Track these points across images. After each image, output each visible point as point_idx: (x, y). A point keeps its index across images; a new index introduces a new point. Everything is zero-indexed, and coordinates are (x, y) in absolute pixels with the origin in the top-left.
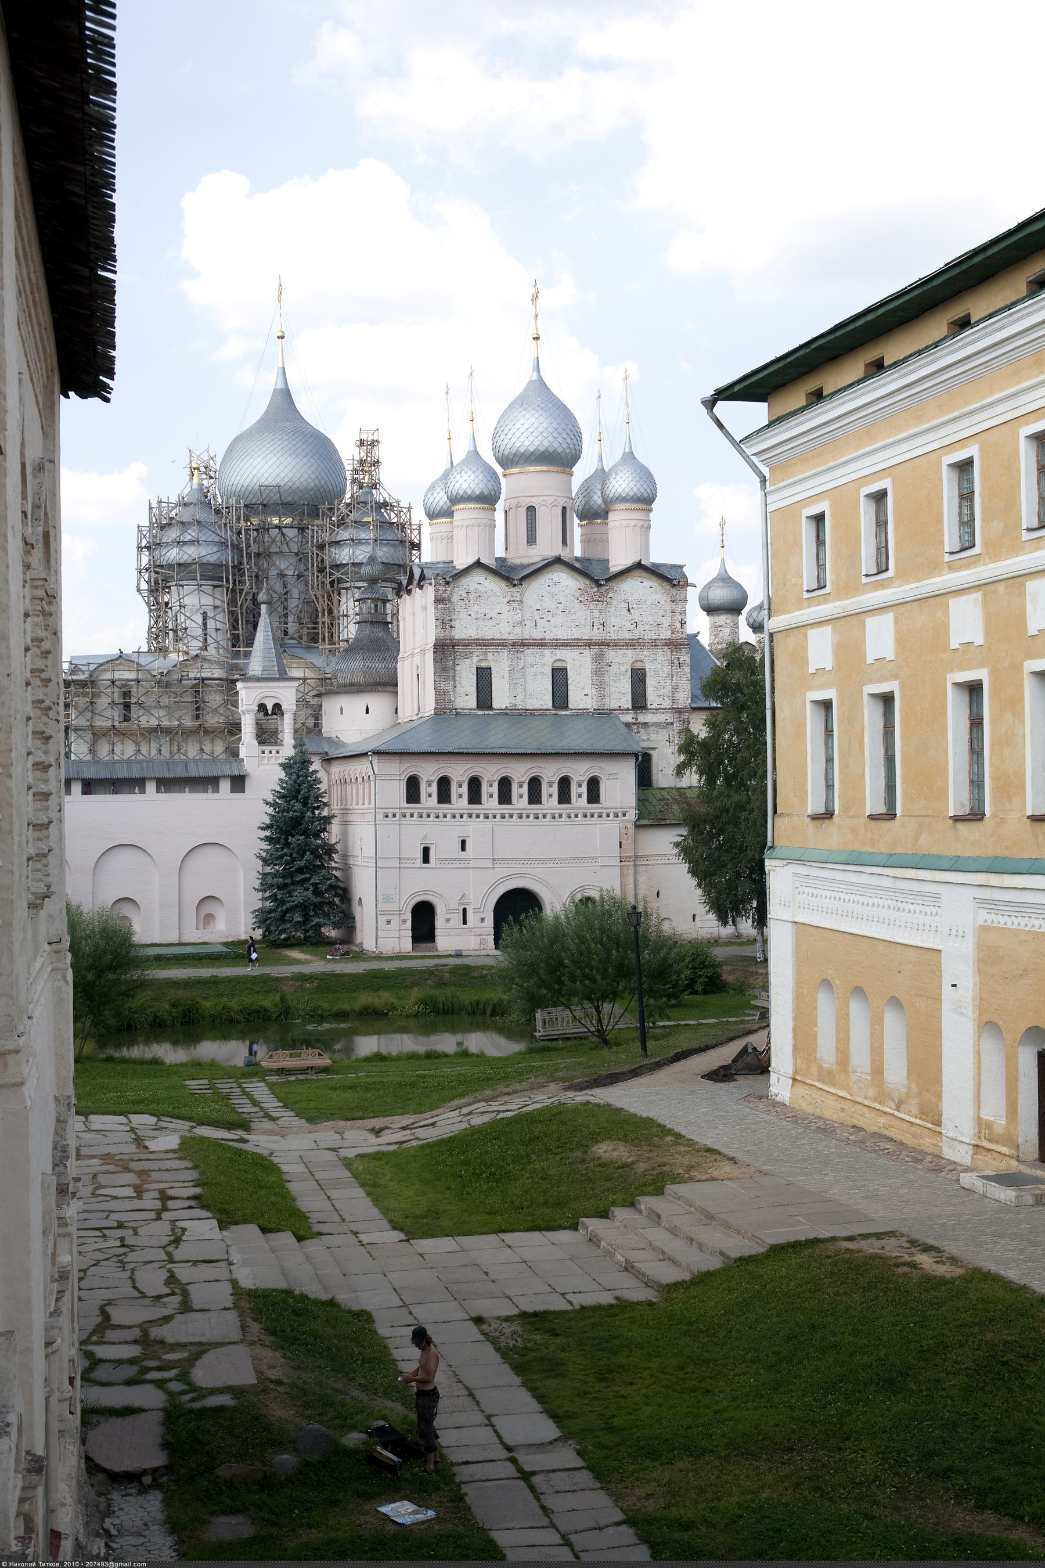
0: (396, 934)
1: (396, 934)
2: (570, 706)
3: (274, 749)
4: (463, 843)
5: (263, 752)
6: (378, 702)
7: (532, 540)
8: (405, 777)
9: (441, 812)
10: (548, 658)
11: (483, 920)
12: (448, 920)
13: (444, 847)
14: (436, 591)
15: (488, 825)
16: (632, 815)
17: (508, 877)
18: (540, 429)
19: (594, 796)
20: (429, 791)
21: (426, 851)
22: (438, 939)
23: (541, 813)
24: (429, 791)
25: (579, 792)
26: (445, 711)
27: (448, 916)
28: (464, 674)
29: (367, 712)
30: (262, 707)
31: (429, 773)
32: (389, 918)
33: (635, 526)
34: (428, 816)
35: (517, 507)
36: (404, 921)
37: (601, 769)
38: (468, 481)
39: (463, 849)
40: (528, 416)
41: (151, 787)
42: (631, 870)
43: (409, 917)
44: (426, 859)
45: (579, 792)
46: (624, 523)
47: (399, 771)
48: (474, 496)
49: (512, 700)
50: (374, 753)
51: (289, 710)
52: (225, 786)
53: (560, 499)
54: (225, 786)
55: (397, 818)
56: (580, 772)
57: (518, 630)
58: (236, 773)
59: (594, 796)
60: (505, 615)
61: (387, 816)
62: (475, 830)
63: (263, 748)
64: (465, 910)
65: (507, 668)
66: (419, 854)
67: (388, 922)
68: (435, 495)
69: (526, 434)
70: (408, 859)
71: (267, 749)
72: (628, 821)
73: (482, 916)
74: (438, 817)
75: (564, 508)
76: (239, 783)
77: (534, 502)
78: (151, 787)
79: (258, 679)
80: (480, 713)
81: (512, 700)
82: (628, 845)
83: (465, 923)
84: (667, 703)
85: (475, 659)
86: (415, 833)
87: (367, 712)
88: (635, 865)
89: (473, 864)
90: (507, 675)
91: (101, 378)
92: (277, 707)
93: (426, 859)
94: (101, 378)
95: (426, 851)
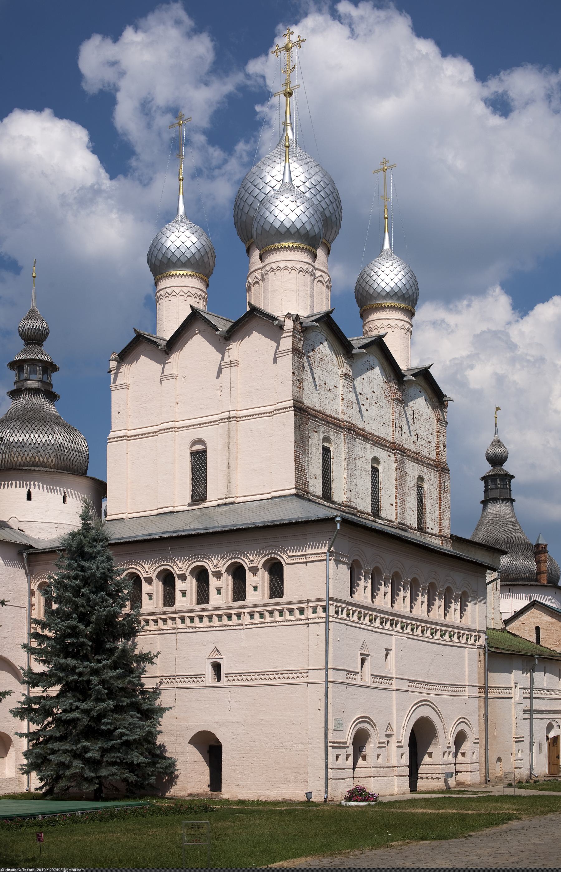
2: (382, 514)
10: (370, 452)
14: (294, 337)
26: (302, 494)
28: (314, 451)
46: (400, 324)
49: (348, 495)
57: (349, 412)
60: (340, 390)
65: (344, 456)
80: (326, 504)
81: (348, 495)
84: (436, 531)
85: (322, 436)
89: (395, 684)
90: (344, 464)
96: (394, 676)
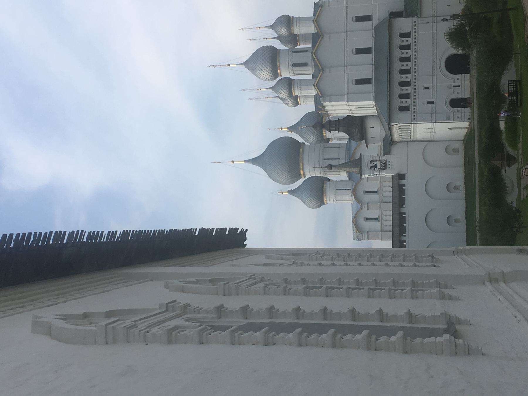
0: (463, 114)
1: (463, 114)
3: (388, 163)
4: (426, 88)
6: (370, 123)
7: (305, 65)
8: (399, 112)
9: (413, 97)
11: (458, 79)
12: (458, 93)
13: (427, 96)
16: (415, 19)
18: (263, 62)
20: (406, 102)
21: (429, 103)
23: (414, 57)
24: (406, 102)
25: (405, 41)
27: (456, 93)
30: (371, 168)
31: (398, 102)
32: (456, 117)
34: (415, 102)
35: (293, 71)
36: (458, 111)
37: (396, 33)
39: (428, 88)
41: (403, 210)
42: (438, 18)
44: (432, 103)
45: (405, 41)
47: (396, 114)
52: (403, 182)
54: (403, 182)
56: (398, 41)
58: (397, 178)
59: (407, 35)
62: (420, 84)
63: (388, 168)
64: (454, 87)
66: (430, 106)
71: (388, 166)
72: (418, 21)
74: (415, 99)
75: (293, 52)
76: (401, 177)
77: (291, 64)
78: (403, 210)
79: (361, 169)
82: (427, 20)
83: (459, 86)
88: (436, 16)
91: (214, 234)
92: (371, 162)
93: (432, 103)
94: (214, 234)
95: (429, 103)
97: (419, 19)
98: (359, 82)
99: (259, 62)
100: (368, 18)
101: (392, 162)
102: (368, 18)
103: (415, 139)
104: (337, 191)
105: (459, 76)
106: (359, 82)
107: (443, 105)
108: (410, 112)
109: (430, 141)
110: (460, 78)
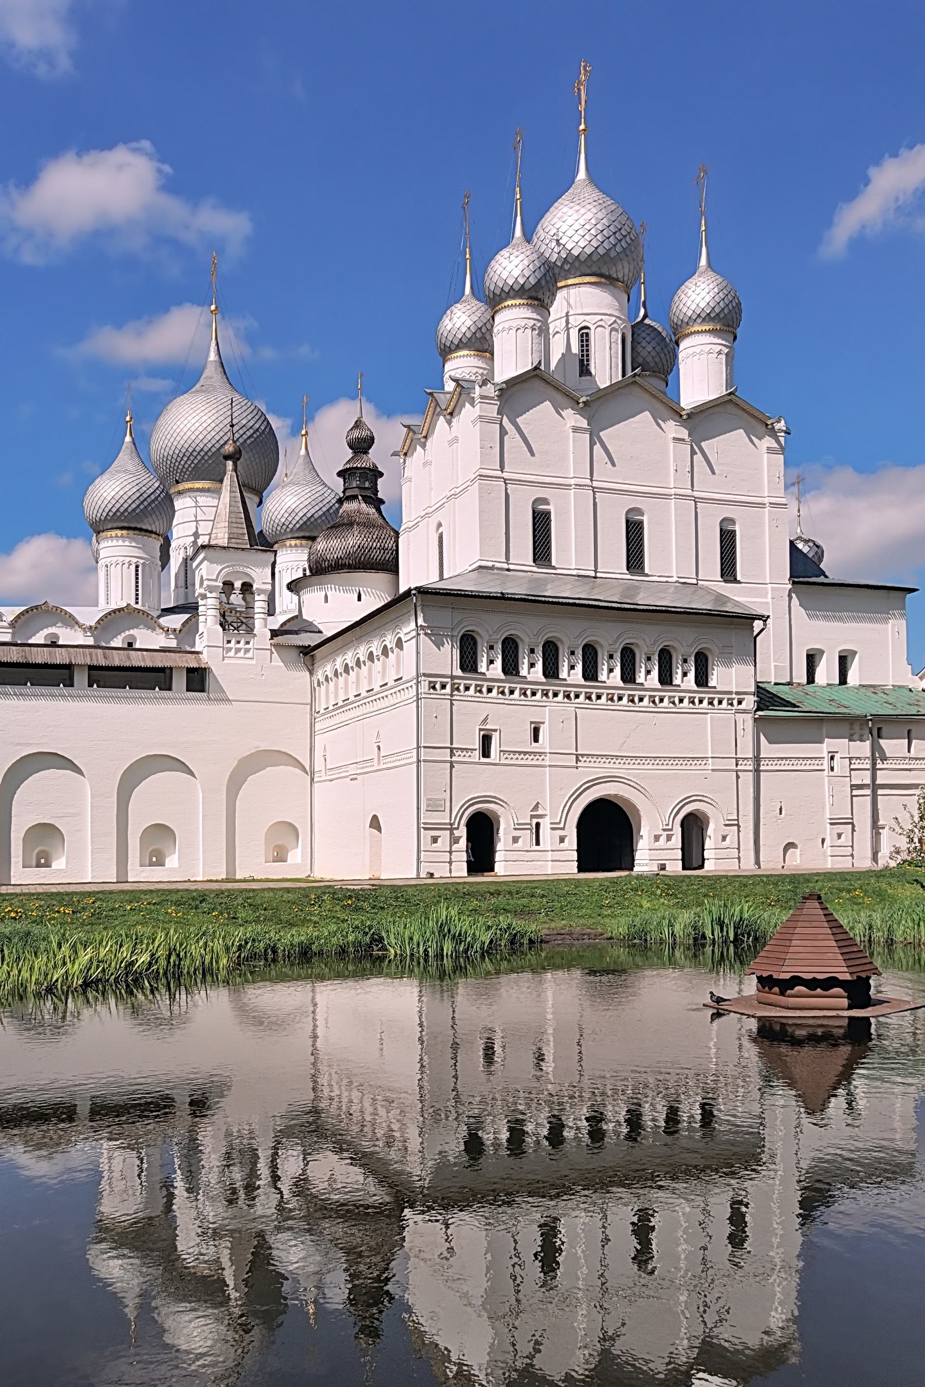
5: (229, 642)
11: (562, 840)
12: (515, 840)
13: (511, 735)
15: (569, 708)
17: (596, 782)
18: (600, 227)
19: (702, 680)
21: (486, 741)
22: (496, 869)
29: (359, 599)
33: (719, 353)
34: (490, 690)
38: (521, 267)
39: (536, 740)
40: (583, 211)
43: (462, 832)
44: (486, 753)
48: (527, 286)
50: (419, 592)
51: (261, 591)
53: (619, 322)
55: (448, 689)
59: (702, 680)
61: (434, 688)
62: (552, 713)
64: (538, 825)
66: (477, 744)
67: (435, 840)
68: (455, 319)
69: (581, 232)
70: (462, 749)
73: (562, 833)
77: (590, 321)
83: (538, 843)
86: (474, 712)
87: (359, 599)
95: (486, 741)
96: (548, 751)
97: (749, 718)
98: (541, 523)
99: (600, 215)
100: (728, 571)
101: (247, 651)
102: (728, 571)
103: (318, 726)
104: (133, 567)
105: (572, 842)
106: (541, 523)
107: (475, 785)
108: (459, 673)
109: (312, 773)
110: (565, 845)
